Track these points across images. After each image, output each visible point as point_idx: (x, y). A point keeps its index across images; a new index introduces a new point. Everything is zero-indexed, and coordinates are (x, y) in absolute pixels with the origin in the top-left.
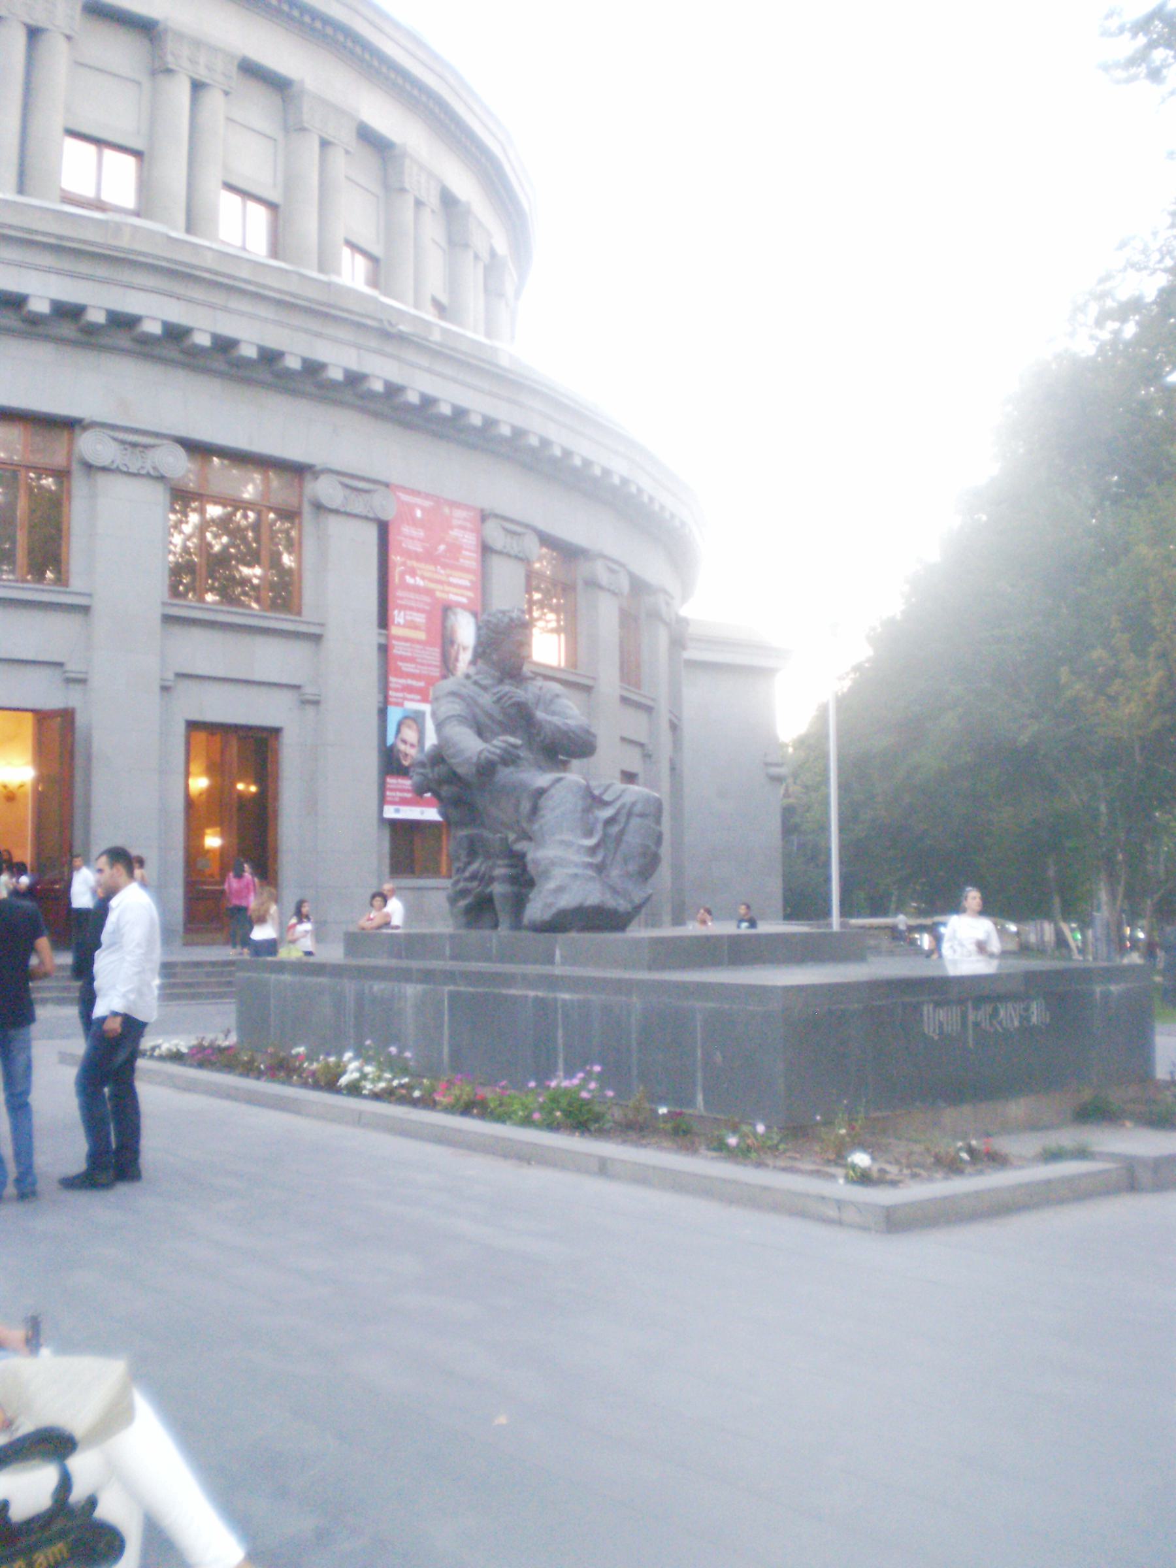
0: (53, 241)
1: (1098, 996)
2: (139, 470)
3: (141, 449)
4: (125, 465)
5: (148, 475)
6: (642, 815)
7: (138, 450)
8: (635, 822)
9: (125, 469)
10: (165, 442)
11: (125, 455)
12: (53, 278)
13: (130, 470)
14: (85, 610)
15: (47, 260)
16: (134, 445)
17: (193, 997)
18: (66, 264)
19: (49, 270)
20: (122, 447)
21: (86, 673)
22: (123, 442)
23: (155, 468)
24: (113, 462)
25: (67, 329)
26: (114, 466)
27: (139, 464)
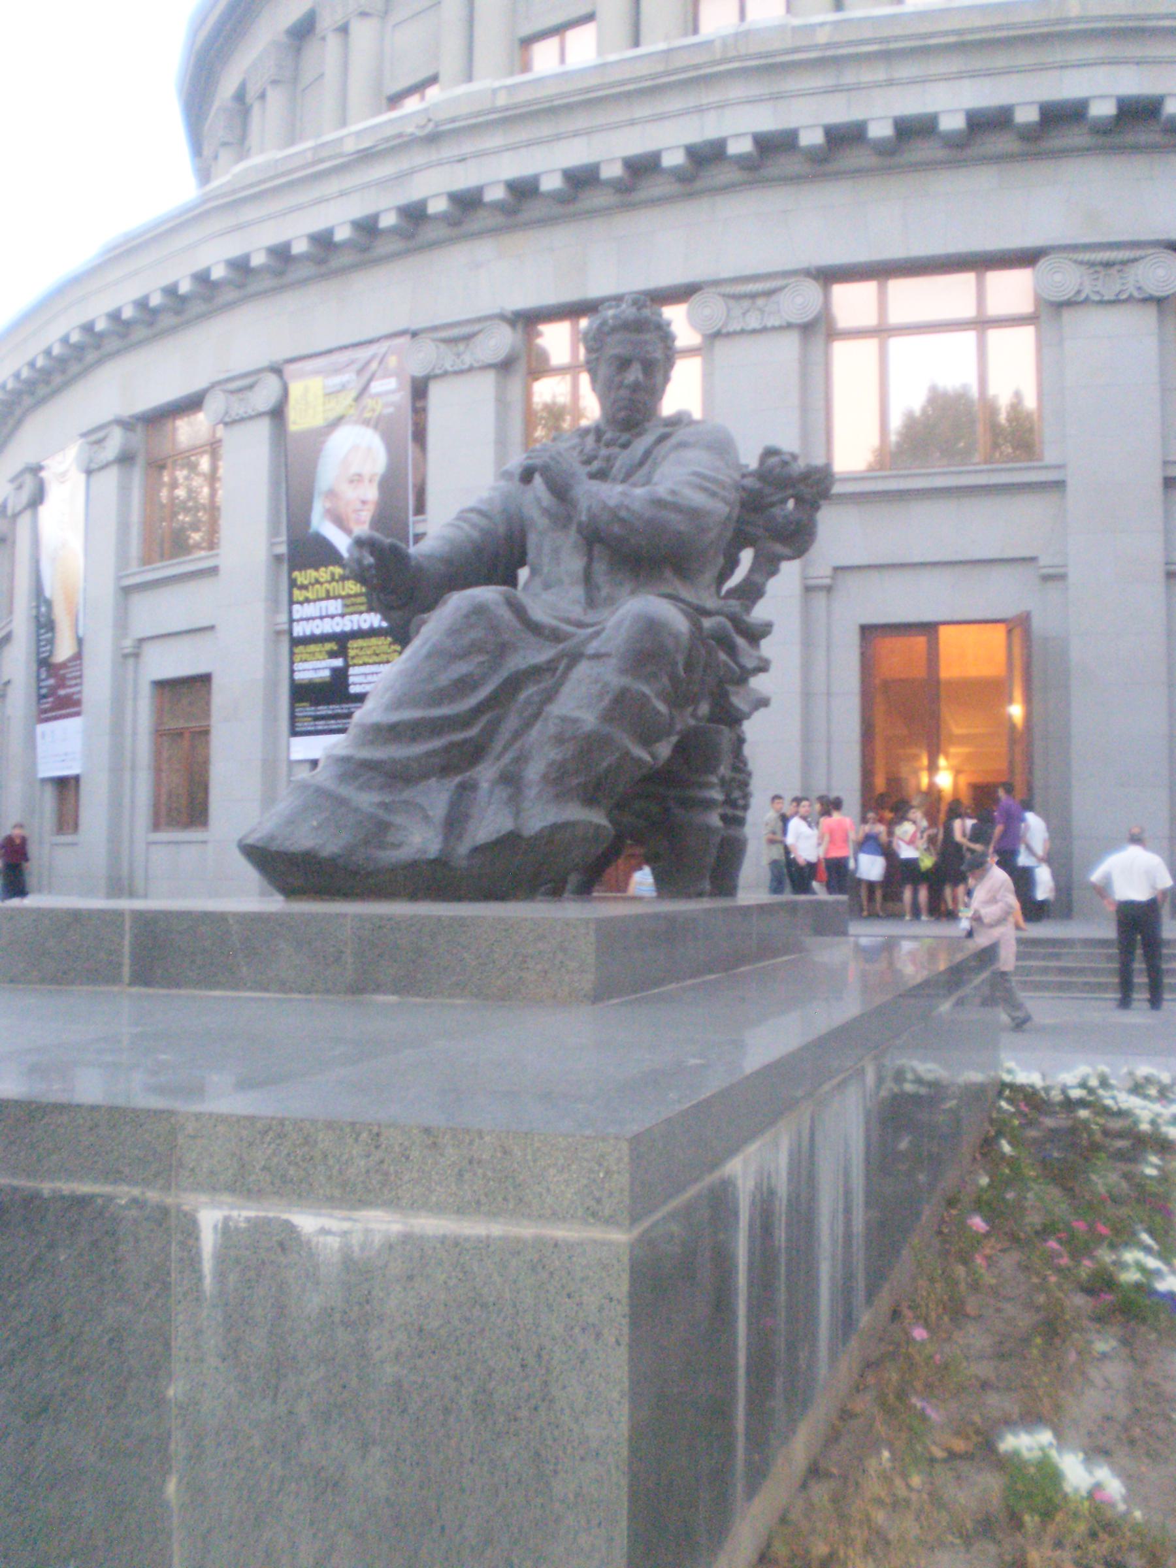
0: (952, 39)
1: (208, 1241)
2: (1117, 295)
3: (1117, 267)
4: (1097, 293)
5: (1130, 299)
6: (597, 656)
7: (1113, 271)
8: (583, 669)
9: (1096, 298)
10: (1150, 251)
11: (1096, 279)
12: (966, 83)
13: (1106, 298)
14: (1058, 486)
15: (955, 64)
16: (1108, 265)
17: (1061, 987)
18: (979, 62)
19: (960, 76)
20: (1092, 270)
21: (1064, 566)
22: (1091, 264)
23: (1139, 289)
24: (1079, 292)
25: (1005, 143)
26: (1082, 297)
27: (1118, 288)
